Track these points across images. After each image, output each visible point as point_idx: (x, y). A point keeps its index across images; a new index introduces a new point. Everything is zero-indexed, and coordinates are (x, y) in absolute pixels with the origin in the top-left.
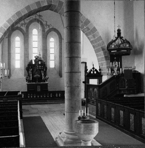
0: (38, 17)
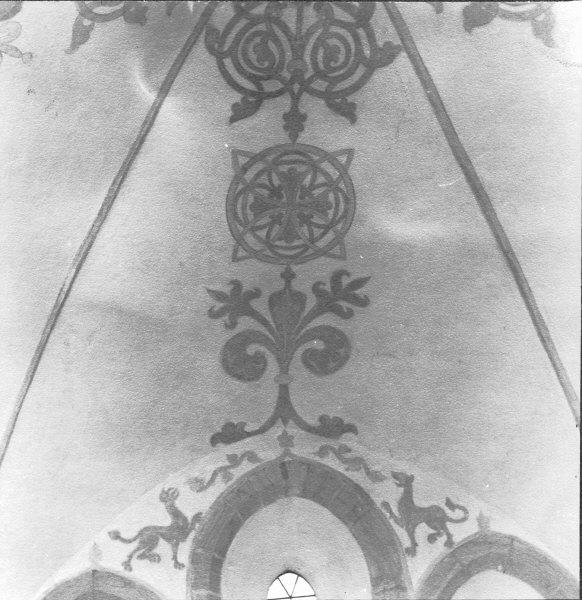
0: (305, 448)
